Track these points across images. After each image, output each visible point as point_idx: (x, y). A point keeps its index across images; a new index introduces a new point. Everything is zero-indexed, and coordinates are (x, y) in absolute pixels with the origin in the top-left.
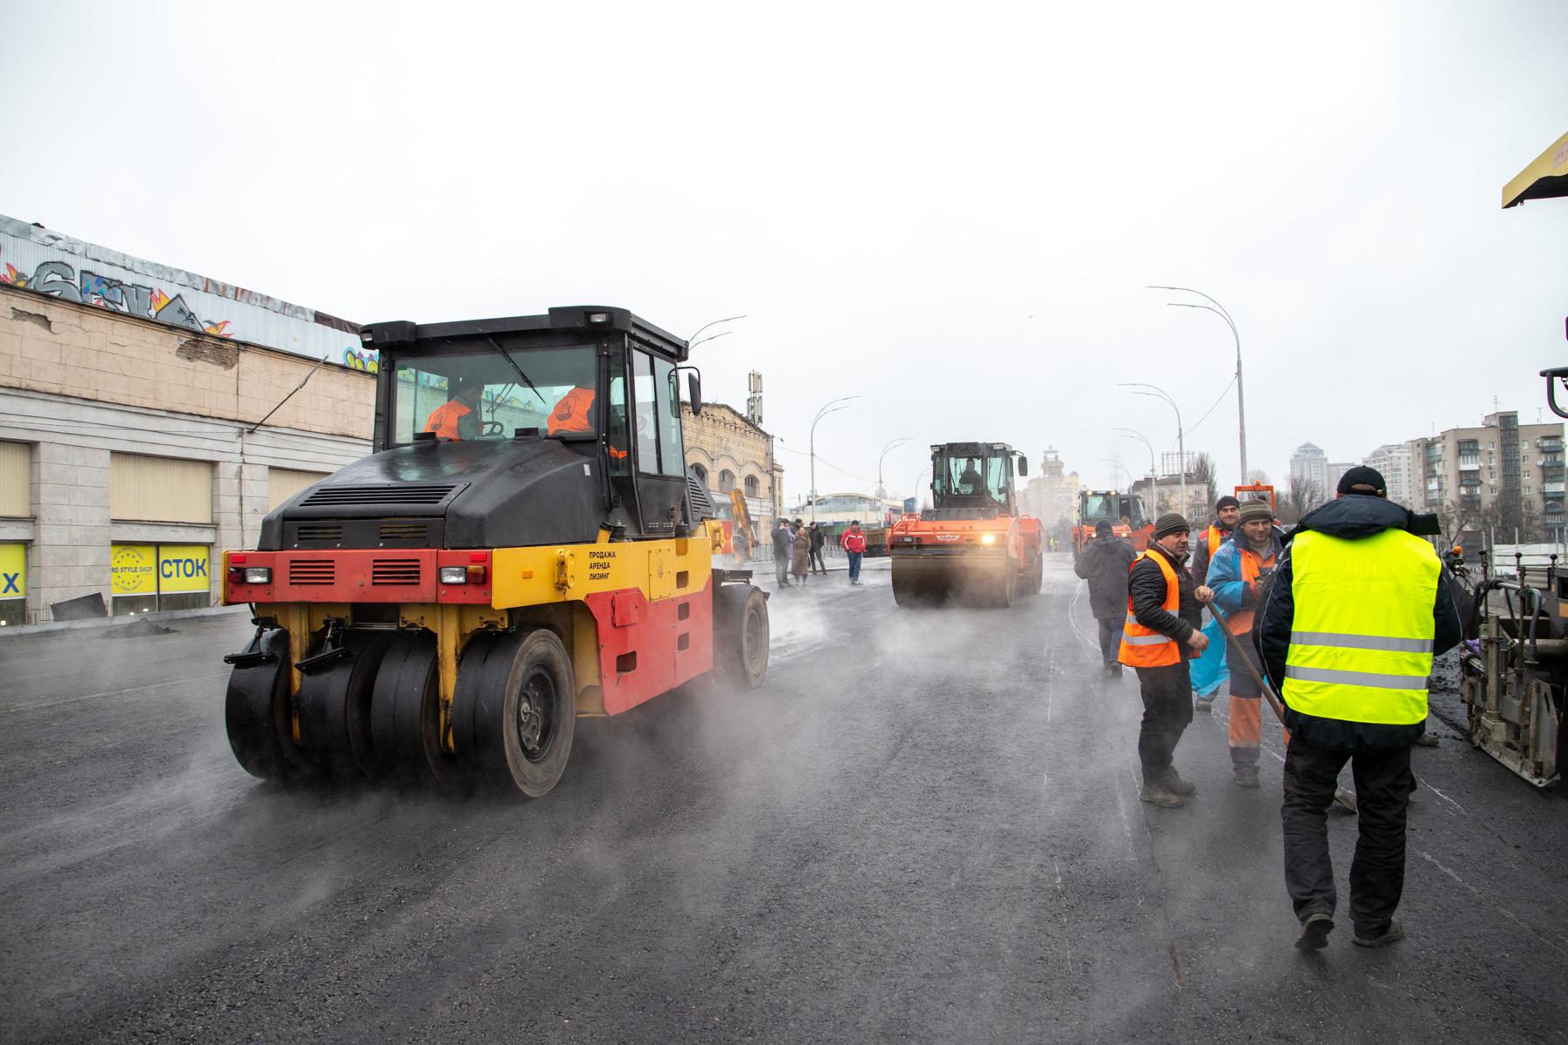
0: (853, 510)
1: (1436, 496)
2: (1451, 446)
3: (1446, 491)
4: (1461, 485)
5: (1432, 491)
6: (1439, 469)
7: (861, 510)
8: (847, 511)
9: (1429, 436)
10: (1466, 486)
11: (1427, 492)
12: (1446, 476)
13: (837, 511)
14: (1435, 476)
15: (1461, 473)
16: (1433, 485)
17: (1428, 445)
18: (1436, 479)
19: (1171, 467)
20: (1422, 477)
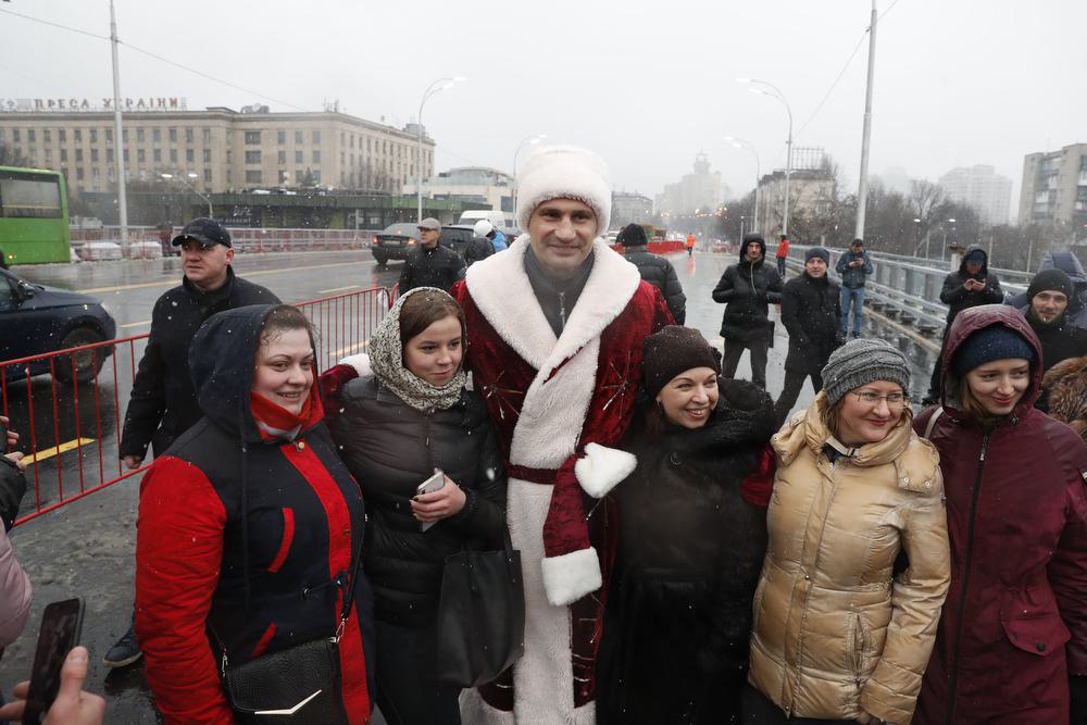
0: (476, 184)
1: (1044, 209)
2: (1073, 160)
3: (1059, 205)
4: (1077, 200)
5: (1040, 204)
6: (1052, 183)
7: (484, 184)
8: (469, 184)
9: (1045, 150)
10: (1082, 201)
11: (1035, 204)
12: (1061, 190)
13: (460, 183)
14: (1047, 190)
15: (1079, 187)
16: (1044, 198)
17: (1044, 159)
18: (1048, 193)
19: (795, 162)
20: (1032, 191)
